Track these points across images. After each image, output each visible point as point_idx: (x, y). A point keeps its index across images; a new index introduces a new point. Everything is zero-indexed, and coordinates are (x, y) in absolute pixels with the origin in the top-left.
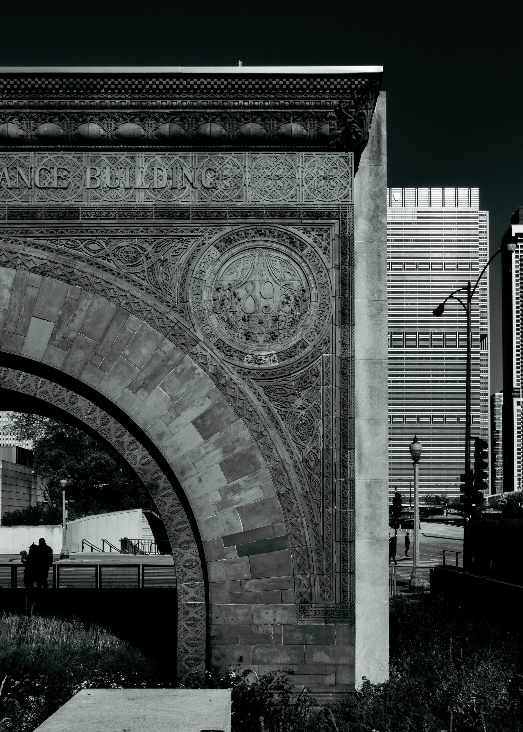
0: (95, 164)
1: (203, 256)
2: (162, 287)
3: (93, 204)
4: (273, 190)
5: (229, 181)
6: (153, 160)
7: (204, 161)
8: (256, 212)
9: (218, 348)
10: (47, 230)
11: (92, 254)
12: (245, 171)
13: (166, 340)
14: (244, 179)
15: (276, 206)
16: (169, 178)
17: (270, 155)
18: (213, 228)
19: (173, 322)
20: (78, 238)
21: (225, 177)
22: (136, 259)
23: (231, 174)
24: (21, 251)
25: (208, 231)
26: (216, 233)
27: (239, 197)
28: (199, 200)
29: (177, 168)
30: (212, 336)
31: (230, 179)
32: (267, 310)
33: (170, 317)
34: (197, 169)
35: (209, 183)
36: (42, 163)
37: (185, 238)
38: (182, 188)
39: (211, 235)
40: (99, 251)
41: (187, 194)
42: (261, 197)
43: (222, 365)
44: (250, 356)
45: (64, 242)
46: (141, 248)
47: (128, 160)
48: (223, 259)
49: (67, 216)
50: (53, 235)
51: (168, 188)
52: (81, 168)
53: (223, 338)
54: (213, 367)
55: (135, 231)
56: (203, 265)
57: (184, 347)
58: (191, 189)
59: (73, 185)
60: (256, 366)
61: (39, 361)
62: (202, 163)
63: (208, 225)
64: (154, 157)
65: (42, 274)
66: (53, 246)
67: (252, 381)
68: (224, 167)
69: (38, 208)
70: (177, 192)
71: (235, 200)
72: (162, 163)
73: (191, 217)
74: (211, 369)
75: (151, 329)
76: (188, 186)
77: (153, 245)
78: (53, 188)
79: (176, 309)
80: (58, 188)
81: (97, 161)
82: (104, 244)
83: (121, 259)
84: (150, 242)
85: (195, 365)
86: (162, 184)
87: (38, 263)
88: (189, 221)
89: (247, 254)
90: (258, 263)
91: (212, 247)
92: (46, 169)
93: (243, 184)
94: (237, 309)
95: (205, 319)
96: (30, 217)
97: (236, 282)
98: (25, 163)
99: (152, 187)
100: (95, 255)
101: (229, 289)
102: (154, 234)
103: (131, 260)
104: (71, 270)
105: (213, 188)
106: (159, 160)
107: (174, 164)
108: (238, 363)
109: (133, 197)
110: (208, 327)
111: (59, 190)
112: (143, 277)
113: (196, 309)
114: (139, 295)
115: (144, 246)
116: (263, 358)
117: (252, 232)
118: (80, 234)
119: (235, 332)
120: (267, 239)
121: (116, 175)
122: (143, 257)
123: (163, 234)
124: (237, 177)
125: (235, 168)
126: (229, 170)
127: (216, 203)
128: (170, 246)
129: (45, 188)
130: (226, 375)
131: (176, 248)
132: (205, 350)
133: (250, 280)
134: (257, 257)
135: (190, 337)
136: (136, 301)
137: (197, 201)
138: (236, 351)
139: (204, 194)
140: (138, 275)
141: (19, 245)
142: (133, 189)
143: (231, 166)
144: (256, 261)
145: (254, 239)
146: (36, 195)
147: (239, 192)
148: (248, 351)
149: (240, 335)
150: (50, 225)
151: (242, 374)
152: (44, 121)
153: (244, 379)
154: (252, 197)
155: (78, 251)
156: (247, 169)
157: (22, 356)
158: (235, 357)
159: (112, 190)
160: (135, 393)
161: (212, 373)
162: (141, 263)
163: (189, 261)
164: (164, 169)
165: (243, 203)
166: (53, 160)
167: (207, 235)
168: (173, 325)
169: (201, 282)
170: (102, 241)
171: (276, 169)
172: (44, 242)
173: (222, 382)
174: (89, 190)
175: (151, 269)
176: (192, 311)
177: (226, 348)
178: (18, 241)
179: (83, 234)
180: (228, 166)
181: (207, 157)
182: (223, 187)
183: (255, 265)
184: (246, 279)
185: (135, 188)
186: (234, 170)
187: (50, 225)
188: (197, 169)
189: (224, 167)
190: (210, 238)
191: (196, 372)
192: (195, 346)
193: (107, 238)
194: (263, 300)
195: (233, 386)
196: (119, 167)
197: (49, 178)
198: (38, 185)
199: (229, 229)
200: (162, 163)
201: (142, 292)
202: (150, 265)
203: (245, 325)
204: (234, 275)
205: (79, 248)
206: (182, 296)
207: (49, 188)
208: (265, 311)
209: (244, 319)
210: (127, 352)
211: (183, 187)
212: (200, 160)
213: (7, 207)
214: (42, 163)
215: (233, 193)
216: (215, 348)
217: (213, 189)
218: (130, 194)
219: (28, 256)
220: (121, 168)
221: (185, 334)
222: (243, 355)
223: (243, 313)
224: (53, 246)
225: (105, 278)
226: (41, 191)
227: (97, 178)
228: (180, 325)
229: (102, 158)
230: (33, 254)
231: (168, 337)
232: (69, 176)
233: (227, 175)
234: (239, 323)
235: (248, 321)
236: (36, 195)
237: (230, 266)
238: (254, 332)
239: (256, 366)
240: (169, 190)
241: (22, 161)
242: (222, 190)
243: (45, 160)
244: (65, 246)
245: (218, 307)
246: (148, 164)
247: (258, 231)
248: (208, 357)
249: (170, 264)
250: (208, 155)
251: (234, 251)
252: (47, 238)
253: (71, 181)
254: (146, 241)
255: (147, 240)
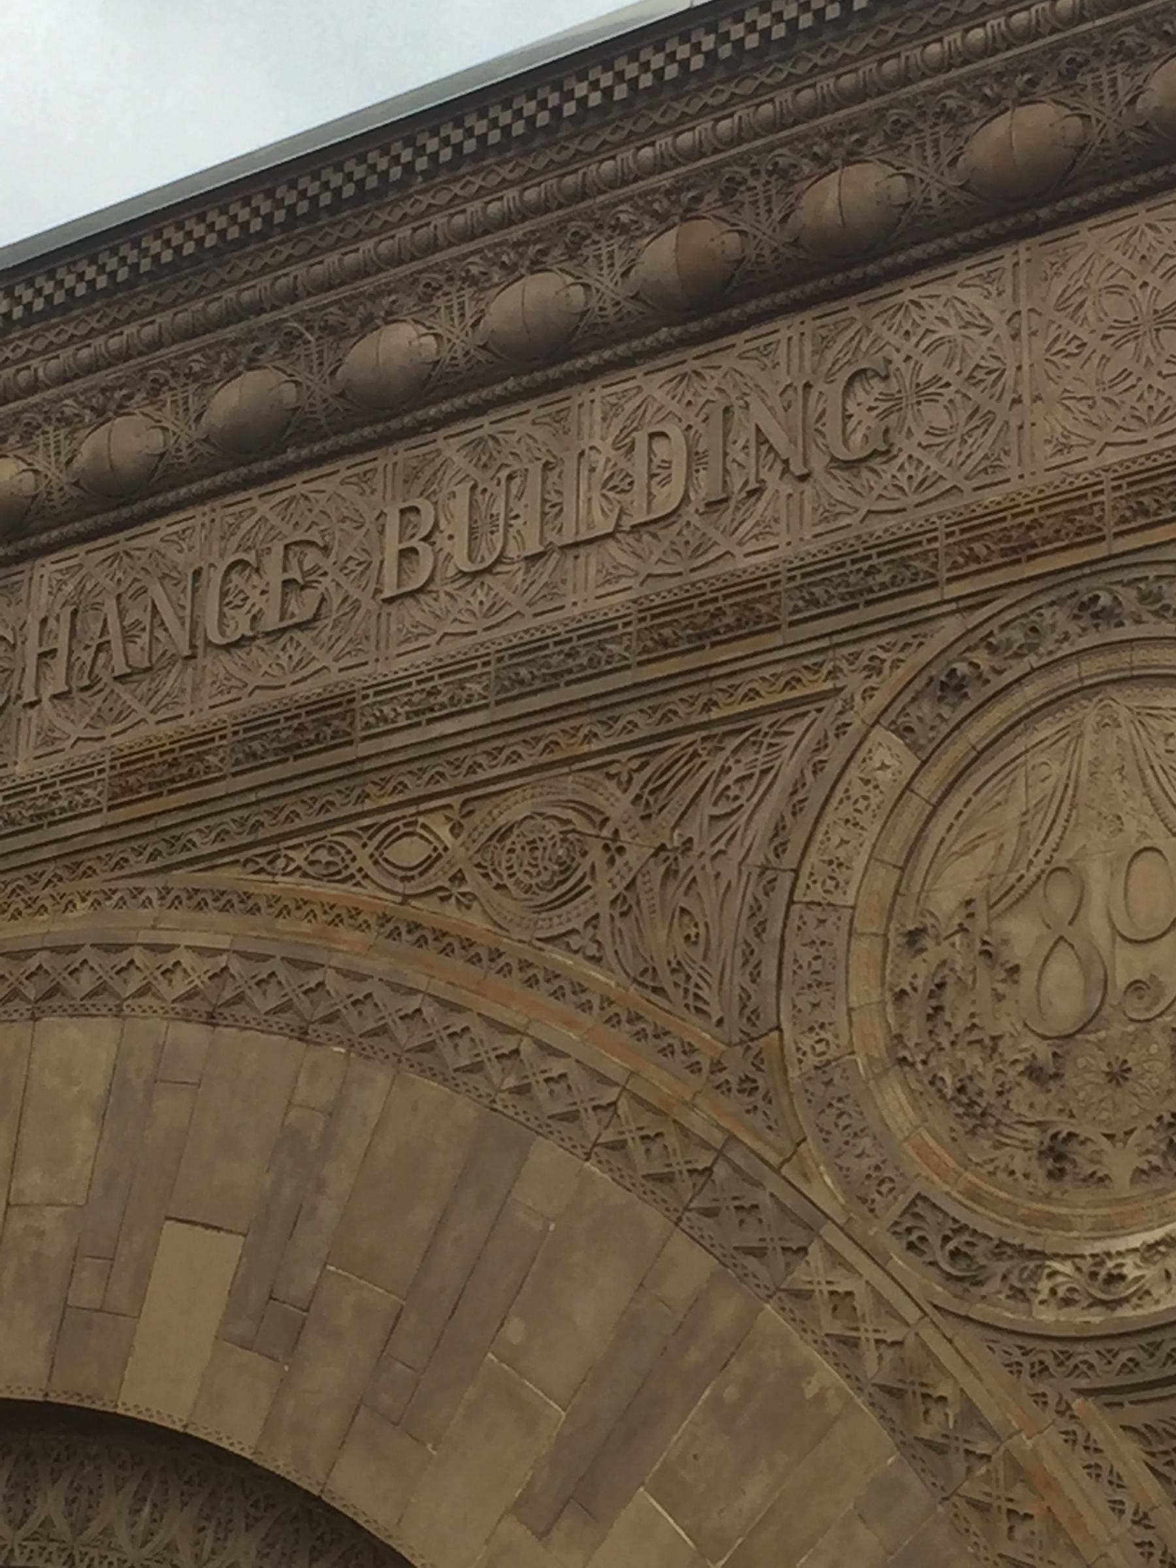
0: (417, 488)
1: (841, 787)
2: (666, 979)
3: (404, 662)
4: (1143, 384)
5: (943, 401)
6: (637, 401)
7: (838, 346)
8: (1068, 516)
9: (911, 1246)
10: (242, 822)
11: (399, 887)
12: (1015, 336)
13: (680, 1242)
14: (1010, 373)
15: (1162, 460)
16: (695, 459)
17: (1125, 225)
18: (883, 641)
19: (707, 1146)
20: (352, 826)
21: (924, 393)
22: (566, 869)
23: (956, 367)
24: (145, 937)
25: (864, 660)
26: (896, 664)
27: (991, 464)
28: (819, 529)
29: (727, 410)
30: (884, 1189)
31: (949, 393)
32: (1146, 1001)
33: (696, 1122)
34: (808, 386)
35: (857, 439)
36: (234, 541)
37: (766, 721)
38: (751, 493)
39: (874, 681)
40: (429, 863)
41: (769, 514)
42: (1093, 433)
43: (929, 1334)
44: (1067, 1268)
45: (299, 857)
46: (587, 810)
47: (540, 433)
48: (928, 786)
49: (310, 742)
50: (262, 834)
51: (691, 509)
52: (370, 516)
53: (939, 1190)
54: (889, 1354)
55: (563, 740)
56: (841, 832)
57: (752, 1263)
58: (787, 488)
59: (336, 601)
60: (1096, 1317)
61: (178, 1427)
62: (830, 356)
63: (860, 633)
64: (639, 388)
65: (211, 1020)
66: (262, 886)
67: (1077, 1403)
68: (924, 344)
69: (204, 739)
70: (726, 518)
71: (976, 483)
72: (674, 406)
73: (784, 617)
74: (872, 1365)
75: (619, 1197)
76: (772, 478)
77: (631, 794)
78: (268, 634)
79: (724, 1076)
80: (284, 630)
81: (428, 472)
82: (444, 832)
83: (509, 883)
84: (624, 777)
85: (808, 1351)
86: (667, 497)
87: (198, 971)
88: (776, 639)
89: (1046, 729)
90: (1096, 763)
91: (879, 734)
92: (244, 564)
93: (1008, 397)
94: (1004, 1026)
95: (848, 1106)
96: (183, 778)
97: (996, 882)
98: (180, 559)
99: (627, 524)
100: (410, 888)
101: (962, 929)
102: (637, 735)
103: (545, 877)
104: (313, 979)
105: (875, 453)
106: (658, 394)
107: (717, 396)
108: (1009, 1314)
109: (551, 591)
110: (866, 1143)
111: (287, 636)
112: (592, 950)
113: (811, 1060)
114: (566, 1037)
115: (599, 801)
116: (1130, 1272)
117: (1060, 617)
118: (359, 808)
119: (999, 1145)
120: (1130, 631)
121: (494, 512)
122: (597, 855)
123: (676, 724)
124: (980, 375)
125: (974, 332)
126: (944, 349)
127: (891, 521)
128: (704, 773)
129: (237, 644)
130: (945, 1390)
131: (728, 780)
132: (851, 1269)
133: (1060, 860)
134: (1090, 736)
135: (782, 1207)
136: (557, 1067)
137: (808, 537)
138: (1001, 1249)
139: (839, 495)
140: (575, 943)
141: (143, 911)
142: (556, 556)
143: (953, 331)
144: (1088, 754)
145: (1067, 649)
146: (209, 681)
147: (988, 440)
148: (1051, 1240)
149: (1018, 1165)
150: (252, 798)
151: (1026, 1368)
152: (231, 372)
153: (1040, 1399)
154: (1049, 449)
155: (347, 886)
156: (1024, 324)
157: (121, 1411)
158: (994, 1285)
159: (476, 583)
160: (543, 1535)
161: (882, 1388)
162: (587, 882)
163: (779, 828)
164: (675, 431)
165: (1006, 488)
166: (274, 519)
167: (854, 682)
168: (704, 1160)
169: (832, 919)
170: (439, 816)
171: (1154, 280)
172: (234, 872)
173: (926, 1432)
174: (392, 609)
175: (624, 905)
176: (793, 1073)
177: (946, 1239)
178: (141, 891)
179: (368, 805)
180: (942, 331)
181: (853, 319)
182: (920, 437)
183: (1085, 776)
184: (1040, 864)
185: (564, 548)
186: (969, 346)
187: (252, 798)
188: (808, 386)
189: (924, 344)
190: (869, 693)
191: (810, 1391)
192: (803, 1250)
193: (455, 800)
194: (1124, 952)
195: (982, 1448)
196: (503, 474)
197: (255, 596)
198: (217, 639)
199: (951, 627)
200: (674, 406)
201: (587, 1020)
202: (620, 889)
203: (1041, 1099)
204: (987, 850)
205: (353, 869)
206: (751, 1006)
207: (253, 638)
208: (1136, 1008)
209: (1034, 1072)
210: (515, 1331)
211: (753, 485)
212: (820, 350)
213: (108, 757)
214: (234, 541)
215: (966, 452)
216: (895, 1248)
217: (875, 463)
218: (545, 578)
219: (168, 948)
220: (510, 477)
221: (763, 1198)
222: (1032, 1265)
223: (1029, 1042)
224: (262, 886)
225: (439, 988)
226: (224, 657)
227: (422, 547)
228: (736, 1156)
229: (447, 453)
230: (186, 939)
231: (684, 1224)
232: (327, 564)
233: (936, 379)
234: (1017, 1094)
235: (1057, 1076)
236: (209, 681)
237: (967, 811)
238: (1083, 1131)
239: (1096, 1317)
240: (695, 520)
241: (171, 552)
242: (918, 454)
243: (246, 526)
244: (305, 875)
245: (914, 1032)
246: (615, 430)
247: (1083, 606)
248: (863, 1302)
249: (706, 860)
250: (854, 312)
251: (977, 732)
252: (242, 856)
253: (332, 587)
254: (609, 776)
255: (613, 770)
